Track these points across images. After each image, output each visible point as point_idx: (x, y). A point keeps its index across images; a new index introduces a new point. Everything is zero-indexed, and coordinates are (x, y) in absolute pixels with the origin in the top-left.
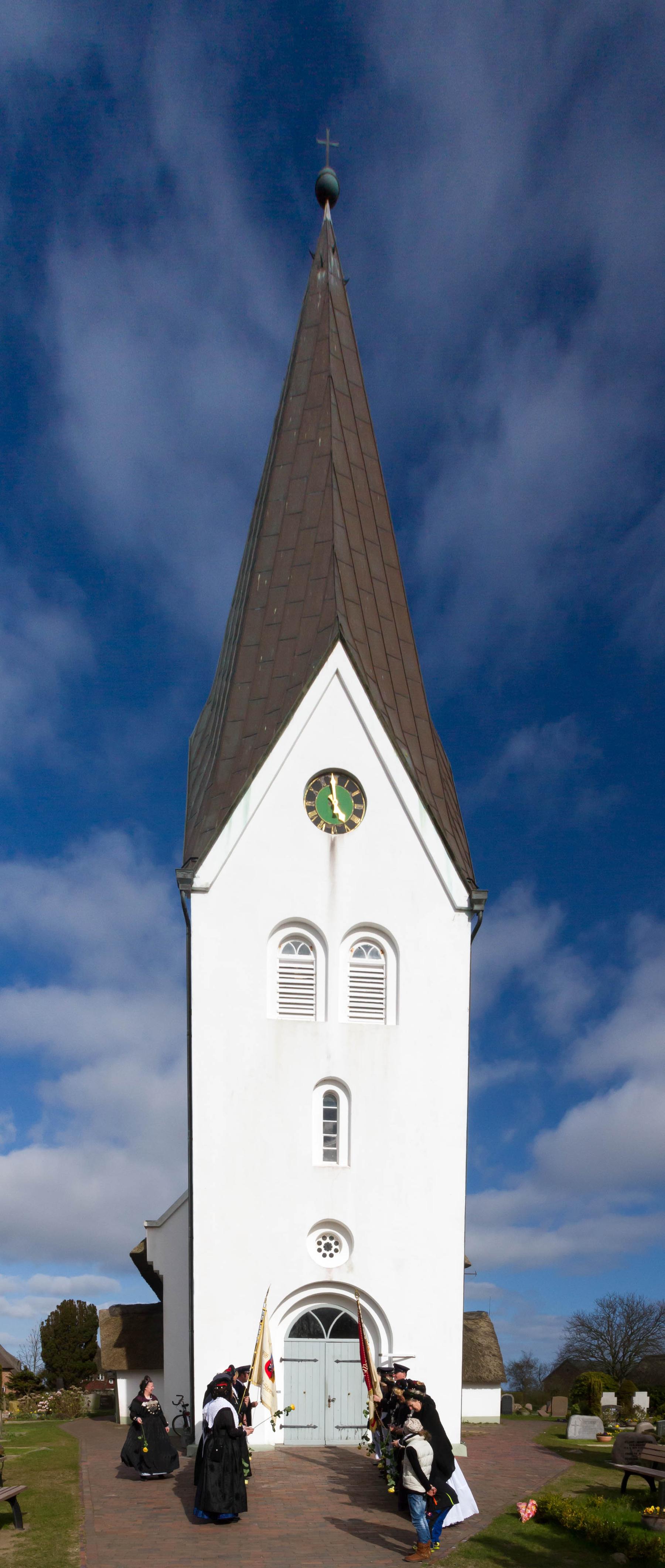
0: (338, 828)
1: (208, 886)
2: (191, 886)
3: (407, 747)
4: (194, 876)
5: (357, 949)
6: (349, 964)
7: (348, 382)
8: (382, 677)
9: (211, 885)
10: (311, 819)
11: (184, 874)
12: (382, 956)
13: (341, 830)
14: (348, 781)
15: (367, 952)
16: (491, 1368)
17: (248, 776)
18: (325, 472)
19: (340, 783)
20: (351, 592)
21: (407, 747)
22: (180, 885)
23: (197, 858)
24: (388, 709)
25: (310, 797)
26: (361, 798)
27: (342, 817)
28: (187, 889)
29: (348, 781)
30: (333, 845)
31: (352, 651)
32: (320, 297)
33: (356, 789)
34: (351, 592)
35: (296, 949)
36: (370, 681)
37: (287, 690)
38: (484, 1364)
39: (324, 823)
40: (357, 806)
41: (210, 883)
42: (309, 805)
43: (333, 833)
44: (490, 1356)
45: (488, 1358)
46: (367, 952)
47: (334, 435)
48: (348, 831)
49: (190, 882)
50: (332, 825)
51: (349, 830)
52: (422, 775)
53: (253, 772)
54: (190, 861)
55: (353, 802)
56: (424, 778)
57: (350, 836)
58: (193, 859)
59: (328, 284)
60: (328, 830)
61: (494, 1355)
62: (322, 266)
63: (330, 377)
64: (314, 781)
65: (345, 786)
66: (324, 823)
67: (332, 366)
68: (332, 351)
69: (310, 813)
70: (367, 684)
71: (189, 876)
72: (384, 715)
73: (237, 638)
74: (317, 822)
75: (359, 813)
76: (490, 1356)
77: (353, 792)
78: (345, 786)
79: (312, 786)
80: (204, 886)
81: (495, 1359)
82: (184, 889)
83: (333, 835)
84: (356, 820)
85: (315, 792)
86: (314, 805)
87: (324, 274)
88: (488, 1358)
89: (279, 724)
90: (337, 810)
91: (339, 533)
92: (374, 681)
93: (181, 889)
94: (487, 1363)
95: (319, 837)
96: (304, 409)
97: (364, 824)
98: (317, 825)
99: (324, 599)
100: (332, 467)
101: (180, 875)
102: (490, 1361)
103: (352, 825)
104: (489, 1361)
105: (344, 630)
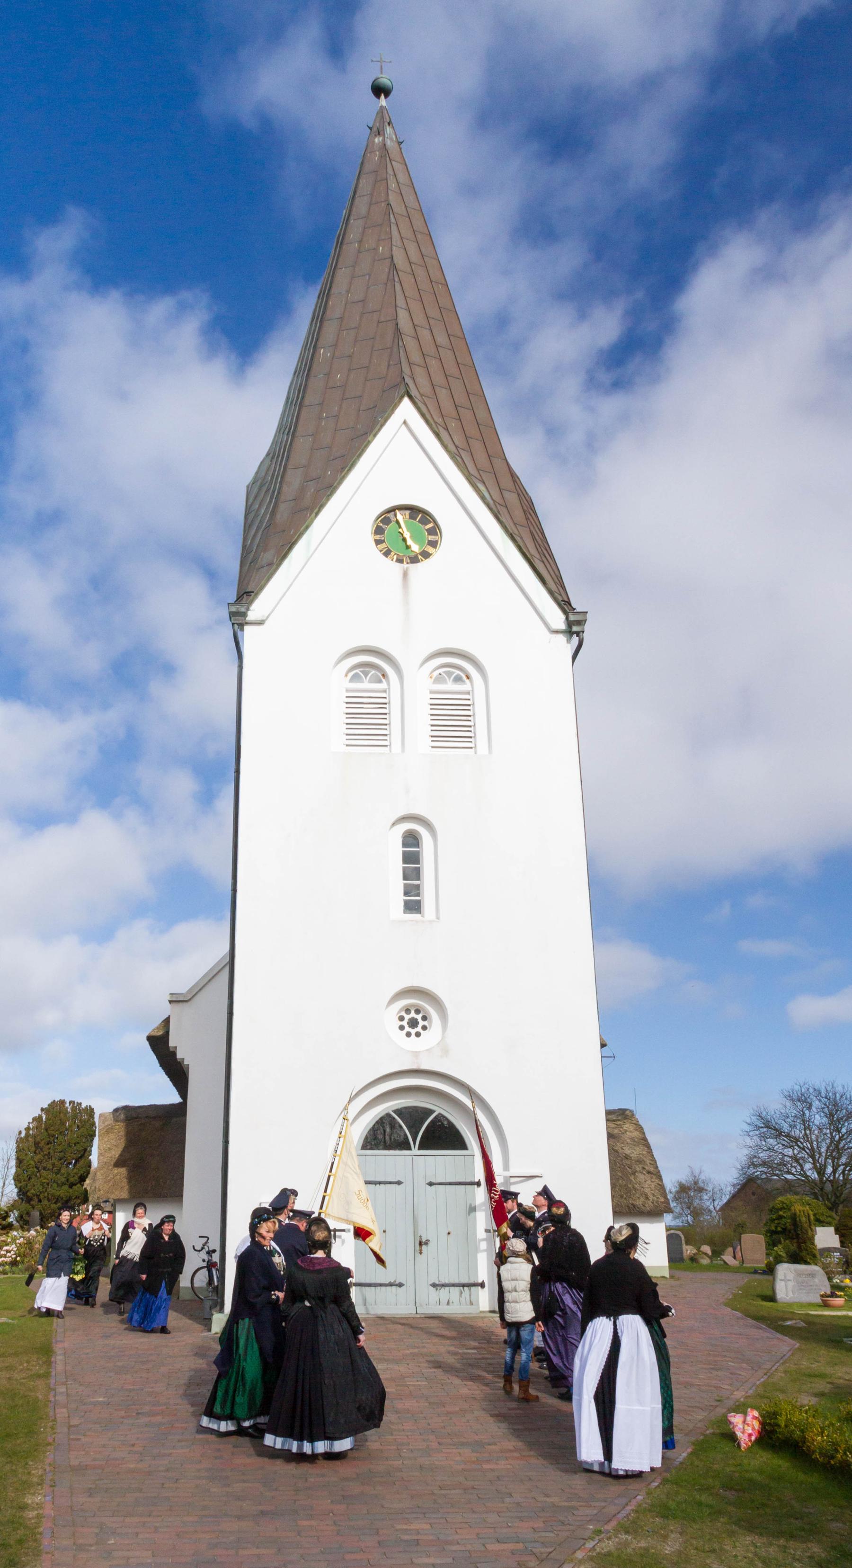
0: (410, 558)
1: (265, 618)
2: (245, 619)
3: (484, 483)
4: (248, 609)
5: (437, 676)
6: (428, 691)
7: (406, 207)
8: (453, 424)
9: (268, 617)
10: (381, 551)
11: (238, 608)
12: (467, 681)
13: (414, 560)
14: (420, 516)
15: (449, 678)
16: (647, 1190)
17: (310, 515)
18: (387, 270)
19: (412, 517)
20: (416, 357)
21: (484, 483)
22: (232, 618)
23: (253, 592)
24: (461, 451)
25: (378, 531)
26: (435, 530)
27: (415, 548)
28: (240, 622)
29: (420, 516)
30: (405, 574)
31: (420, 405)
32: (377, 153)
33: (430, 522)
34: (416, 357)
35: (366, 678)
36: (441, 429)
37: (352, 439)
38: (637, 1186)
39: (395, 554)
40: (431, 538)
41: (266, 615)
42: (378, 538)
43: (405, 563)
44: (644, 1174)
45: (641, 1177)
46: (449, 678)
47: (394, 243)
48: (422, 560)
49: (244, 615)
50: (404, 556)
51: (423, 559)
52: (502, 507)
53: (316, 510)
54: (245, 595)
55: (426, 534)
56: (504, 510)
57: (424, 564)
58: (248, 593)
59: (385, 145)
60: (400, 561)
61: (649, 1172)
62: (379, 134)
63: (389, 205)
64: (383, 517)
65: (417, 520)
66: (395, 554)
67: (391, 197)
68: (390, 188)
69: (379, 546)
70: (437, 430)
71: (243, 610)
72: (457, 457)
73: (299, 399)
74: (387, 553)
75: (434, 544)
76: (644, 1174)
77: (426, 524)
78: (417, 520)
79: (380, 521)
80: (260, 619)
81: (652, 1178)
82: (237, 622)
83: (405, 565)
84: (430, 550)
85: (384, 526)
86: (383, 539)
87: (381, 139)
88: (641, 1177)
89: (343, 469)
90: (410, 542)
91: (403, 315)
92: (445, 429)
93: (233, 622)
94: (640, 1183)
95: (392, 568)
96: (365, 228)
97: (438, 555)
98: (387, 557)
99: (389, 365)
100: (393, 266)
101: (233, 609)
102: (645, 1181)
103: (426, 555)
104: (643, 1181)
105: (410, 386)
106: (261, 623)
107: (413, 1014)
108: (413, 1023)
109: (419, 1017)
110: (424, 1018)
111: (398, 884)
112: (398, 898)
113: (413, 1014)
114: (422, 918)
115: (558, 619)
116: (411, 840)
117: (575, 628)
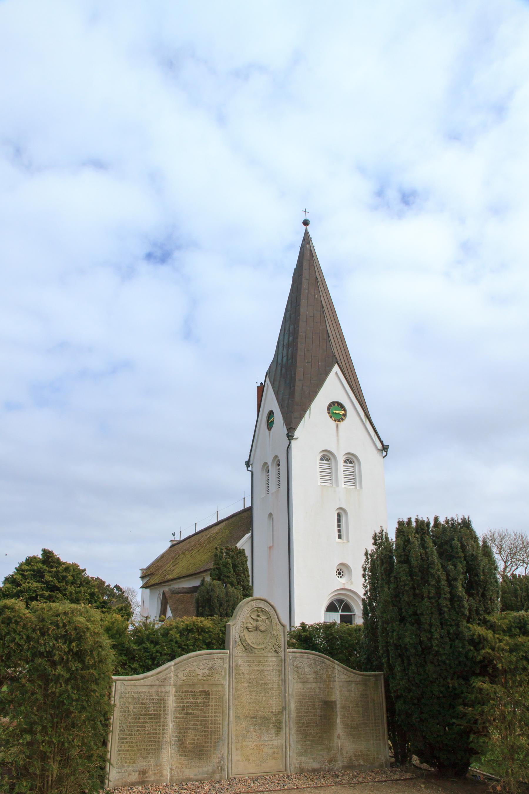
13: (339, 421)
25: (328, 409)
30: (337, 426)
60: (335, 420)
83: (337, 423)
95: (333, 424)
103: (342, 419)
106: (296, 439)
107: (339, 571)
108: (339, 573)
109: (341, 572)
110: (341, 570)
111: (336, 529)
112: (337, 534)
113: (339, 571)
114: (342, 541)
115: (380, 446)
116: (339, 515)
117: (385, 450)
